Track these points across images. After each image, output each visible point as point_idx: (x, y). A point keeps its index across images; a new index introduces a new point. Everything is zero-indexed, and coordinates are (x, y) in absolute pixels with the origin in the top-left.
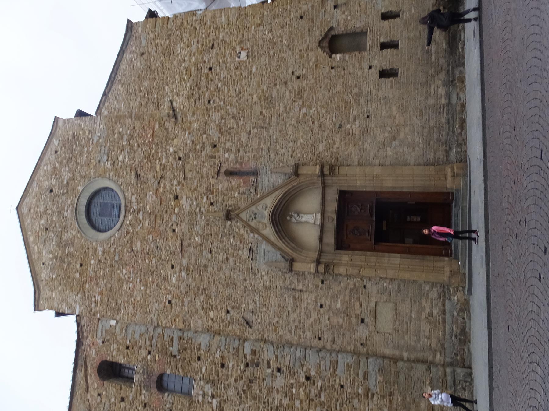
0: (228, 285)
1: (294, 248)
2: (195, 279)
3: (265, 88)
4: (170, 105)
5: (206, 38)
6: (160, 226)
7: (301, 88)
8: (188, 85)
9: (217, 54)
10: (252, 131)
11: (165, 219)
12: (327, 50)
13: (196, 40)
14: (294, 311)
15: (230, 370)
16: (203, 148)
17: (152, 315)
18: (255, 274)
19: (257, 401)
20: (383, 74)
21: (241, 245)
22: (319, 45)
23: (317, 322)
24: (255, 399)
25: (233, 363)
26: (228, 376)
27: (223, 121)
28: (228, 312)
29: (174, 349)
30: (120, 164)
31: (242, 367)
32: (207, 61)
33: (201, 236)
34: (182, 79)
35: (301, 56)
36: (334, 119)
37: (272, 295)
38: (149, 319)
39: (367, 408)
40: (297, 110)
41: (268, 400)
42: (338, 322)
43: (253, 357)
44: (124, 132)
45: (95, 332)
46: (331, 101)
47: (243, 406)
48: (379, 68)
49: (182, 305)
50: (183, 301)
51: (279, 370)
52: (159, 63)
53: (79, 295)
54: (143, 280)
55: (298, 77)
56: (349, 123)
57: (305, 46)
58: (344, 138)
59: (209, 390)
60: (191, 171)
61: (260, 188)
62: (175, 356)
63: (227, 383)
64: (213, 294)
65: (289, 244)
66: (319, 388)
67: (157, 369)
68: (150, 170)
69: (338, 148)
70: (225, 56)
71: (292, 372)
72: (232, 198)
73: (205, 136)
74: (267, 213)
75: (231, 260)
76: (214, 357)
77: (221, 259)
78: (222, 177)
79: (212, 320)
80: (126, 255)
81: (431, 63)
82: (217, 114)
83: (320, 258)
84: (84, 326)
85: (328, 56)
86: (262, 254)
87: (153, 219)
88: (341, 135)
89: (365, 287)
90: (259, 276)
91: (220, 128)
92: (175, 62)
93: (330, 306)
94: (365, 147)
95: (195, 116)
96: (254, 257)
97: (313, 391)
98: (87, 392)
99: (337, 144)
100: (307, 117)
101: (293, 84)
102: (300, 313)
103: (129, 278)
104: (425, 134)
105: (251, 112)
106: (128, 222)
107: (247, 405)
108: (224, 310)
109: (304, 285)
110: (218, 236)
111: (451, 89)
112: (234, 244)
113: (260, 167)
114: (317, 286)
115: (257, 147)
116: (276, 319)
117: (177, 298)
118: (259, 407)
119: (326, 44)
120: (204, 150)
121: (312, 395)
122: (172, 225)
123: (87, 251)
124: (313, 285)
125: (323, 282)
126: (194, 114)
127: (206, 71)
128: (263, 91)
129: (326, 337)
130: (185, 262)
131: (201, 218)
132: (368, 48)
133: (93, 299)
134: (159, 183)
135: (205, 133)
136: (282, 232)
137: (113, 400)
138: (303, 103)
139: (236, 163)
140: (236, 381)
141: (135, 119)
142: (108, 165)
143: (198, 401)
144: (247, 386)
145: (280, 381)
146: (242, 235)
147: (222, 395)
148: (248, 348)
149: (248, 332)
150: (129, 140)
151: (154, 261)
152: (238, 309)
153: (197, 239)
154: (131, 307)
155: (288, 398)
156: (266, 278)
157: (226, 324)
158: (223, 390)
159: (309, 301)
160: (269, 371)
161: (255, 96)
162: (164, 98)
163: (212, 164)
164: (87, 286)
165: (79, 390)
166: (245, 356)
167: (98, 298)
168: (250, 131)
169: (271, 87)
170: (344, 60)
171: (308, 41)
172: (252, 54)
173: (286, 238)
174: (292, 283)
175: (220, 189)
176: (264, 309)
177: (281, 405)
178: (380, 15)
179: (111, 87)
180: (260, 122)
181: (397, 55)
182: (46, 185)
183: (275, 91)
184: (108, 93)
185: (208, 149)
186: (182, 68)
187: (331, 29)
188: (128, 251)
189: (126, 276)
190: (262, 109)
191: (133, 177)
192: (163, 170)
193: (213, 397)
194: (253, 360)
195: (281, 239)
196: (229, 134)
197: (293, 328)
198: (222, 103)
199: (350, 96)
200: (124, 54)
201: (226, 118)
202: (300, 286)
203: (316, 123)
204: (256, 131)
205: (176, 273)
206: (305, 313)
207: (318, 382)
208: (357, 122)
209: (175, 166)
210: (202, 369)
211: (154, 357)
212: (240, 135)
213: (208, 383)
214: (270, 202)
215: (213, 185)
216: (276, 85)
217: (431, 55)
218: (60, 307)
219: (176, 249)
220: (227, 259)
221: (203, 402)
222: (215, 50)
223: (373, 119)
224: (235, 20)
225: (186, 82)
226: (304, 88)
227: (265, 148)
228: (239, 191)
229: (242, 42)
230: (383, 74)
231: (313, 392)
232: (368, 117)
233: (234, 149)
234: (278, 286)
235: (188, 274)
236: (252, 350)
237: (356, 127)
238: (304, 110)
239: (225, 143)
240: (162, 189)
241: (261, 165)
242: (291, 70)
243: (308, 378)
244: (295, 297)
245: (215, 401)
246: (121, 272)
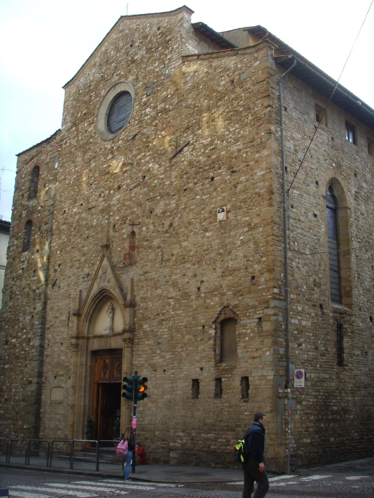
1: (89, 314)
12: (222, 317)
20: (196, 383)
36: (165, 336)
40: (174, 294)
42: (55, 358)
48: (200, 378)
81: (200, 433)
83: (82, 338)
94: (144, 370)
96: (85, 279)
104: (150, 426)
111: (180, 452)
136: (97, 301)
170: (210, 339)
178: (247, 375)
181: (209, 397)
183: (189, 265)
190: (176, 254)
195: (92, 301)
199: (180, 350)
200: (235, 55)
204: (160, 254)
208: (161, 360)
217: (206, 433)
223: (163, 376)
230: (196, 383)
237: (157, 360)
242: (204, 279)
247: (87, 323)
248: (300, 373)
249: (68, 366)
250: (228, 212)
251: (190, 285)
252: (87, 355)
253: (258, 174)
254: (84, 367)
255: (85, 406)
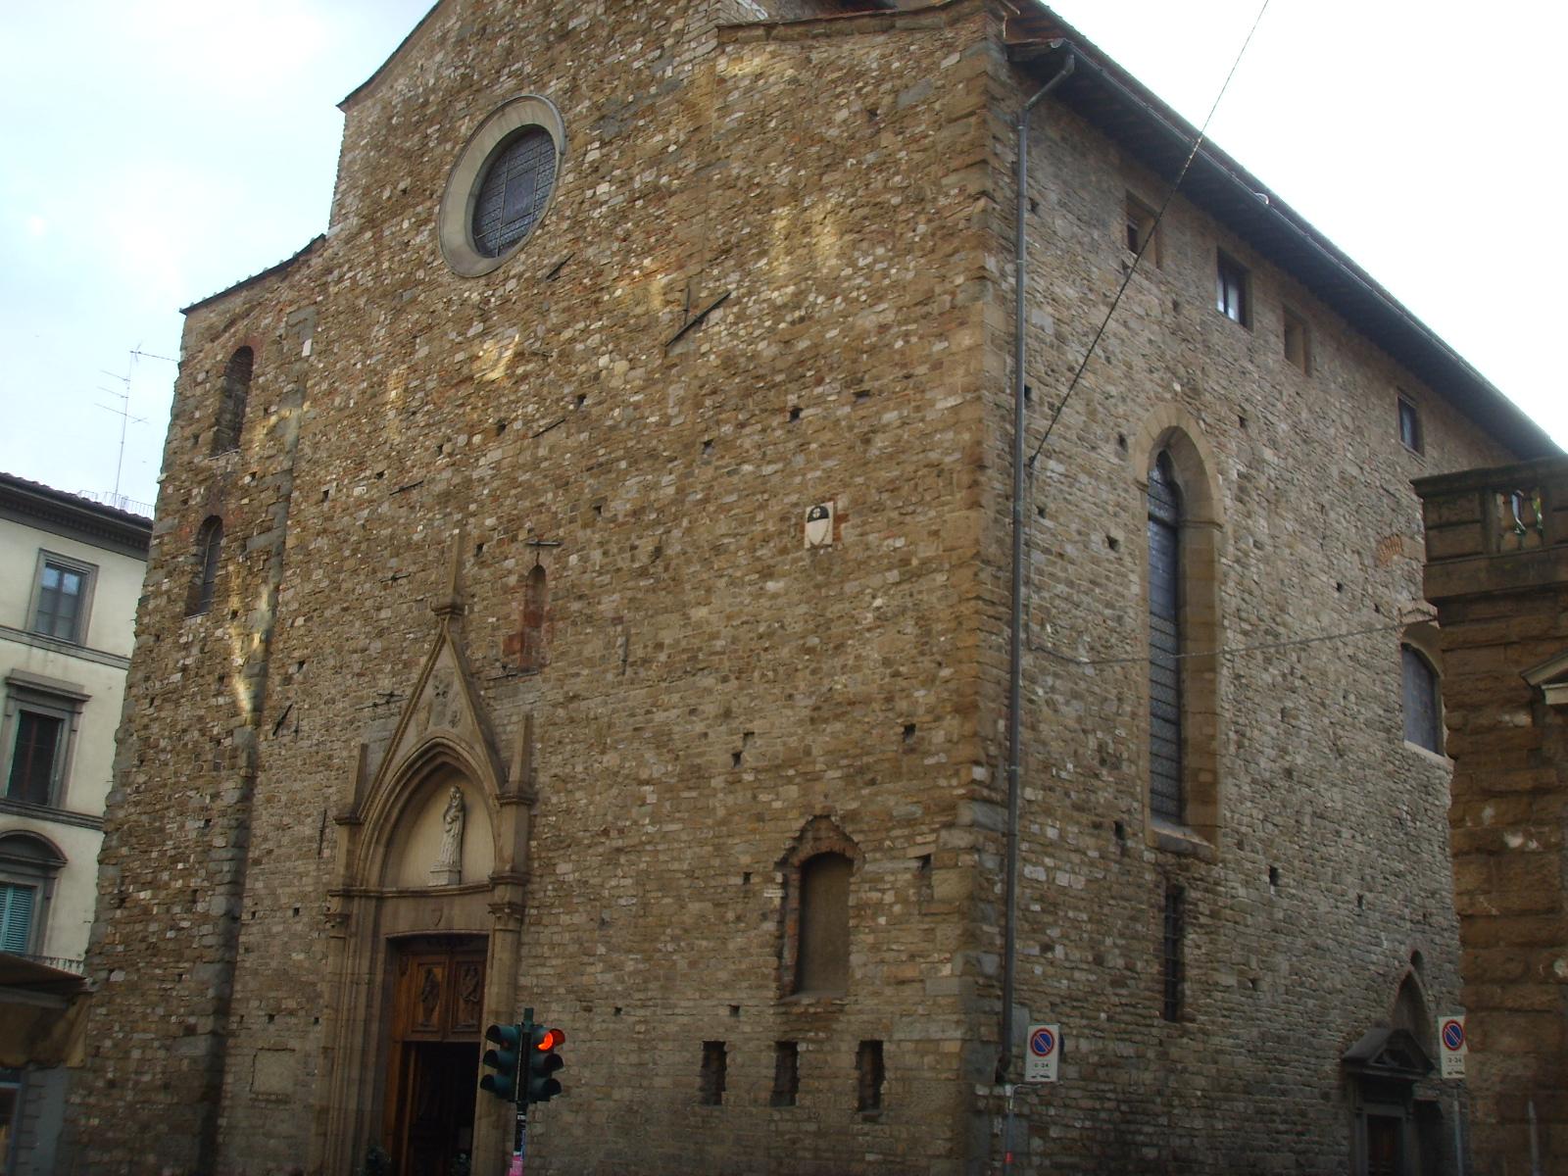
12: (807, 850)
20: (715, 1052)
36: (622, 902)
37: (319, 777)
40: (657, 771)
42: (272, 957)
48: (731, 1038)
65: (392, 806)
94: (554, 1006)
96: (380, 710)
136: (416, 781)
143: (181, 635)
170: (764, 917)
173: (406, 794)
178: (877, 1037)
183: (708, 681)
190: (670, 646)
199: (670, 947)
200: (884, 31)
204: (620, 641)
208: (609, 977)
223: (612, 1026)
230: (715, 1052)
237: (596, 975)
242: (756, 726)
247: (381, 850)
248: (1046, 1036)
249: (314, 984)
250: (840, 519)
251: (710, 745)
252: (374, 951)
253: (940, 405)
254: (364, 988)
255: (360, 1112)
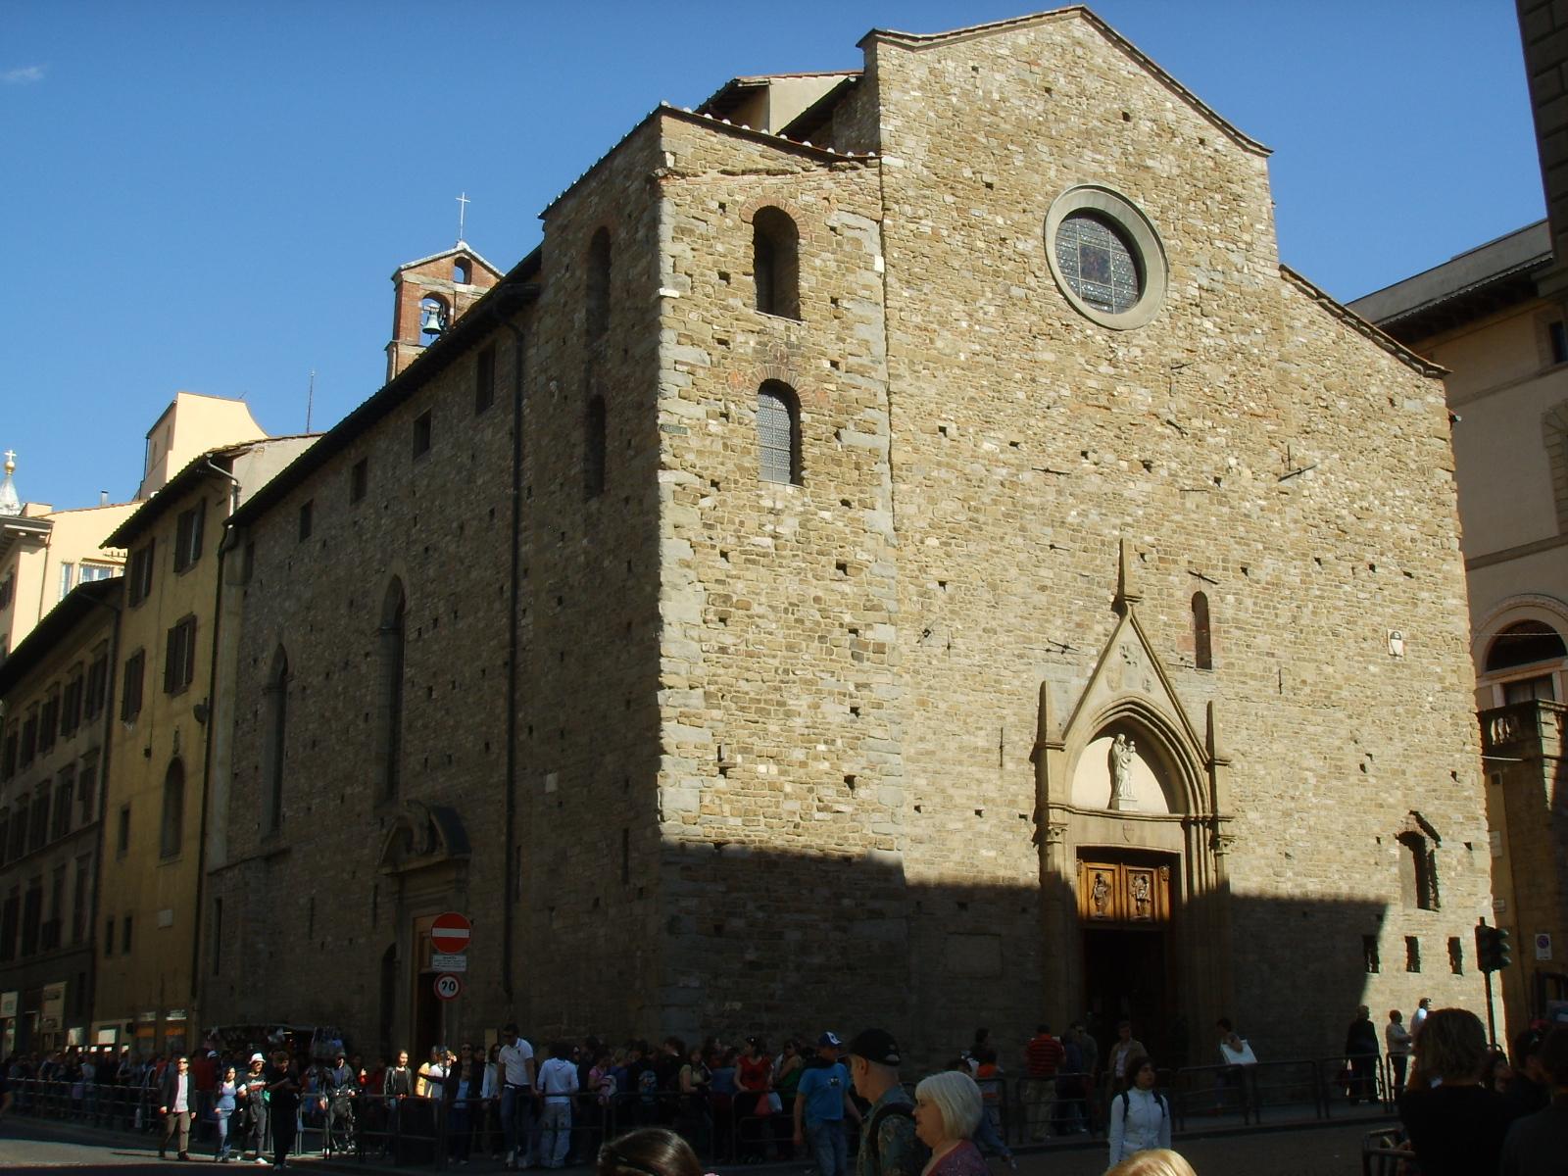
0: (993, 587)
2: (995, 502)
3: (1344, 693)
4: (1309, 464)
5: (1421, 560)
6: (1090, 418)
7: (1346, 772)
8: (1344, 512)
9: (1396, 585)
10: (1273, 660)
11: (1104, 432)
13: (1417, 536)
14: (961, 748)
15: (836, 585)
16: (1241, 541)
17: (908, 379)
18: (1021, 657)
19: (785, 653)
21: (1072, 625)
22: (1411, 813)
23: (948, 803)
24: (790, 648)
25: (851, 596)
26: (822, 578)
27: (1288, 592)
28: (942, 584)
29: (850, 436)
30: (1197, 321)
31: (847, 618)
32: (1384, 559)
33: (1079, 525)
34: (1353, 496)
35: (1395, 772)
37: (987, 696)
38: (903, 369)
39: (816, 917)
40: (1311, 763)
41: (794, 682)
43: (871, 648)
44: (1255, 338)
45: (851, 208)
46: (1327, 838)
47: (772, 616)
49: (939, 464)
50: (948, 466)
51: (854, 710)
52: (1378, 442)
53: (925, 172)
54: (977, 359)
55: (1363, 767)
56: (1297, 874)
57: (1411, 783)
58: (1271, 866)
59: (788, 527)
60: (1197, 507)
61: (1179, 675)
62: (837, 435)
63: (810, 575)
64: (972, 547)
66: (837, 807)
67: (804, 385)
68: (1191, 402)
69: (1254, 852)
70: (1392, 602)
71: (855, 742)
72: (1156, 606)
73: (1260, 546)
74: (1137, 692)
75: (1041, 599)
76: (855, 544)
77: (1043, 572)
78: (1192, 585)
79: (922, 542)
80: (1022, 319)
82: (1298, 580)
84: (860, 176)
85: (1398, 832)
86: (1060, 676)
87: (1103, 400)
88: (1275, 859)
89: (1024, 910)
90: (1019, 665)
91: (1276, 585)
92: (1379, 482)
93: (980, 834)
95: (1292, 526)
96: (1053, 655)
97: (830, 792)
98: (724, 172)
99: (1259, 851)
100: (1301, 786)
101: (1352, 757)
102: (961, 763)
103: (978, 322)
105: (1304, 660)
106: (1089, 332)
107: (774, 626)
108: (944, 576)
109: (1013, 774)
110: (1084, 568)
112: (1073, 607)
113: (1215, 676)
114: (1013, 803)
115: (1248, 670)
116: (943, 706)
117: (953, 451)
118: (774, 657)
119: (1415, 827)
120: (1236, 543)
121: (822, 792)
122: (1095, 452)
123: (1020, 207)
124: (1017, 795)
125: (1021, 816)
126: (1296, 522)
127: (1369, 557)
128: (1339, 687)
129: (922, 822)
130: (1027, 477)
131: (1114, 527)
132: (1407, 912)
133: (921, 212)
134: (1169, 422)
135: (1265, 548)
137: (720, 248)
138: (1324, 777)
139: (1219, 621)
140: (817, 600)
141: (1278, 370)
142: (1193, 291)
144: (811, 630)
145: (835, 713)
146: (1090, 628)
147: (784, 562)
148: (882, 633)
149: (910, 633)
150: (1239, 349)
151: (1021, 395)
152: (952, 612)
153: (1074, 513)
154: (918, 319)
155: (806, 731)
156: (1017, 683)
157: (917, 577)
158: (794, 565)
159: (984, 785)
160: (852, 688)
161: (1330, 670)
162: (1320, 448)
163: (1215, 562)
164: (950, 199)
165: (723, 144)
166: (869, 626)
167: (926, 226)
168: (1273, 655)
169: (1346, 705)
170: (1390, 864)
171: (1418, 789)
172: (1397, 666)
174: (1014, 744)
175: (1171, 578)
176: (958, 677)
177: (788, 714)
179: (1332, 313)
180: (1288, 682)
181: (1398, 970)
182: (1137, 104)
183: (1340, 715)
184: (1322, 305)
185: (1238, 554)
186: (1371, 498)
187: (1436, 838)
188: (1032, 324)
189: (981, 314)
191: (1177, 355)
192: (1194, 436)
193: (775, 536)
194: (865, 646)
196: (1267, 607)
197: (930, 746)
198: (1318, 593)
199: (1336, 877)
201: (1291, 598)
202: (1009, 766)
203: (1293, 805)
204: (1276, 669)
205: (1001, 452)
206: (960, 774)
207: (848, 804)
209: (1205, 468)
210: (828, 510)
211: (827, 379)
212: (1265, 633)
213: (802, 525)
214: (1157, 699)
215: (1175, 562)
216: (1350, 717)
218: (892, 108)
219: (1049, 456)
220: (1043, 588)
221: (760, 509)
222: (1401, 579)
224: (1449, 628)
225: (1348, 506)
226: (1347, 779)
227: (1247, 690)
228: (1170, 626)
229: (1417, 644)
231: (829, 794)
232: (1305, 914)
233: (1242, 615)
234: (1005, 712)
235: (1002, 484)
236: (883, 645)
238: (1312, 781)
239: (1250, 596)
240: (1159, 429)
241: (1219, 679)
243: (850, 780)
244: (988, 751)
245: (769, 541)
246: (990, 302)
248: (1546, 940)
251: (1346, 755)
253: (1450, 601)
